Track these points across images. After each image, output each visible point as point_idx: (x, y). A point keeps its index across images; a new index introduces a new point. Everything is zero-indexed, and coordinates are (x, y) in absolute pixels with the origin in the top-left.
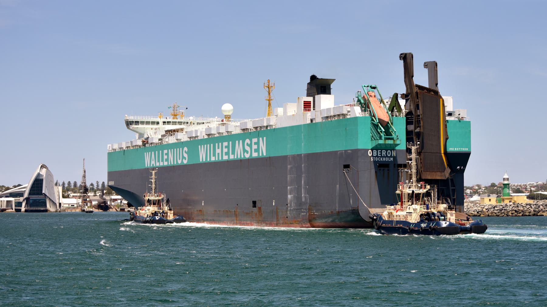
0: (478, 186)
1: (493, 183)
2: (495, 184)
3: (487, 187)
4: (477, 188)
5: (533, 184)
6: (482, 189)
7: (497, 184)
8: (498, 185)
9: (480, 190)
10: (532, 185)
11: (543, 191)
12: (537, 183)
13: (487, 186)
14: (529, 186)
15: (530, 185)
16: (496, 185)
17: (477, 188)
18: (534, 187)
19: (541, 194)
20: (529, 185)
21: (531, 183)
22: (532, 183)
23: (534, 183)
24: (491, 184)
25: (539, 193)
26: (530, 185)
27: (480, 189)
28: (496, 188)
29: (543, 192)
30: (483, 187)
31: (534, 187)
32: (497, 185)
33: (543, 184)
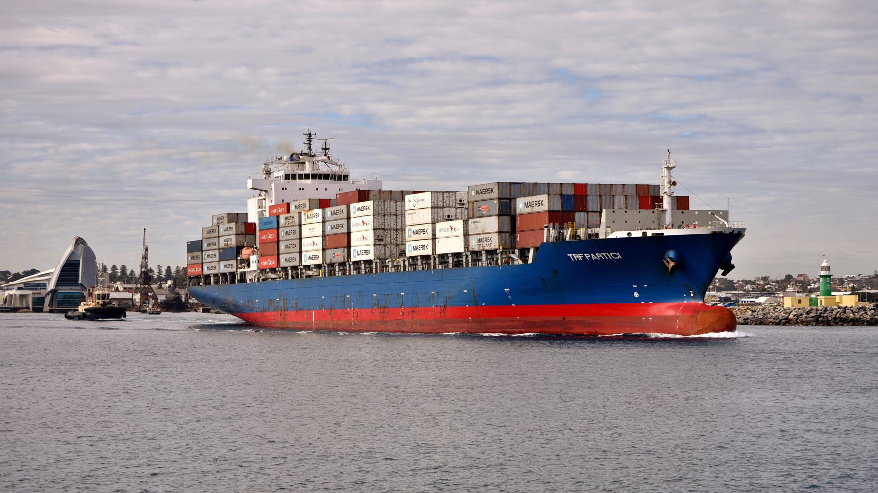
0: (765, 279)
1: (789, 275)
3: (779, 281)
4: (762, 282)
5: (853, 277)
6: (772, 285)
7: (795, 276)
8: (797, 276)
11: (870, 288)
12: (859, 275)
13: (779, 279)
17: (762, 282)
18: (854, 282)
20: (846, 279)
21: (850, 276)
22: (852, 276)
23: (855, 276)
24: (786, 276)
25: (866, 292)
26: (848, 279)
27: (768, 284)
29: (870, 290)
30: (773, 282)
31: (854, 282)
33: (868, 277)
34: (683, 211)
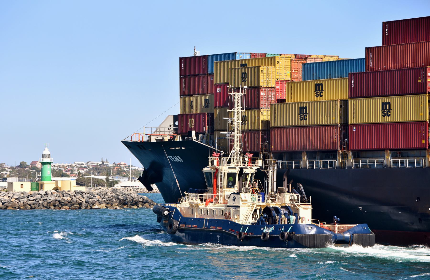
1: (23, 162)
2: (25, 163)
6: (7, 171)
7: (29, 163)
8: (31, 164)
9: (4, 172)
10: (80, 166)
11: (97, 174)
12: (88, 163)
13: (14, 165)
14: (76, 167)
15: (78, 166)
16: (28, 165)
19: (93, 179)
21: (79, 163)
22: (81, 163)
23: (83, 163)
28: (27, 169)
29: (96, 175)
32: (29, 165)
33: (96, 164)
34: (385, 100)
